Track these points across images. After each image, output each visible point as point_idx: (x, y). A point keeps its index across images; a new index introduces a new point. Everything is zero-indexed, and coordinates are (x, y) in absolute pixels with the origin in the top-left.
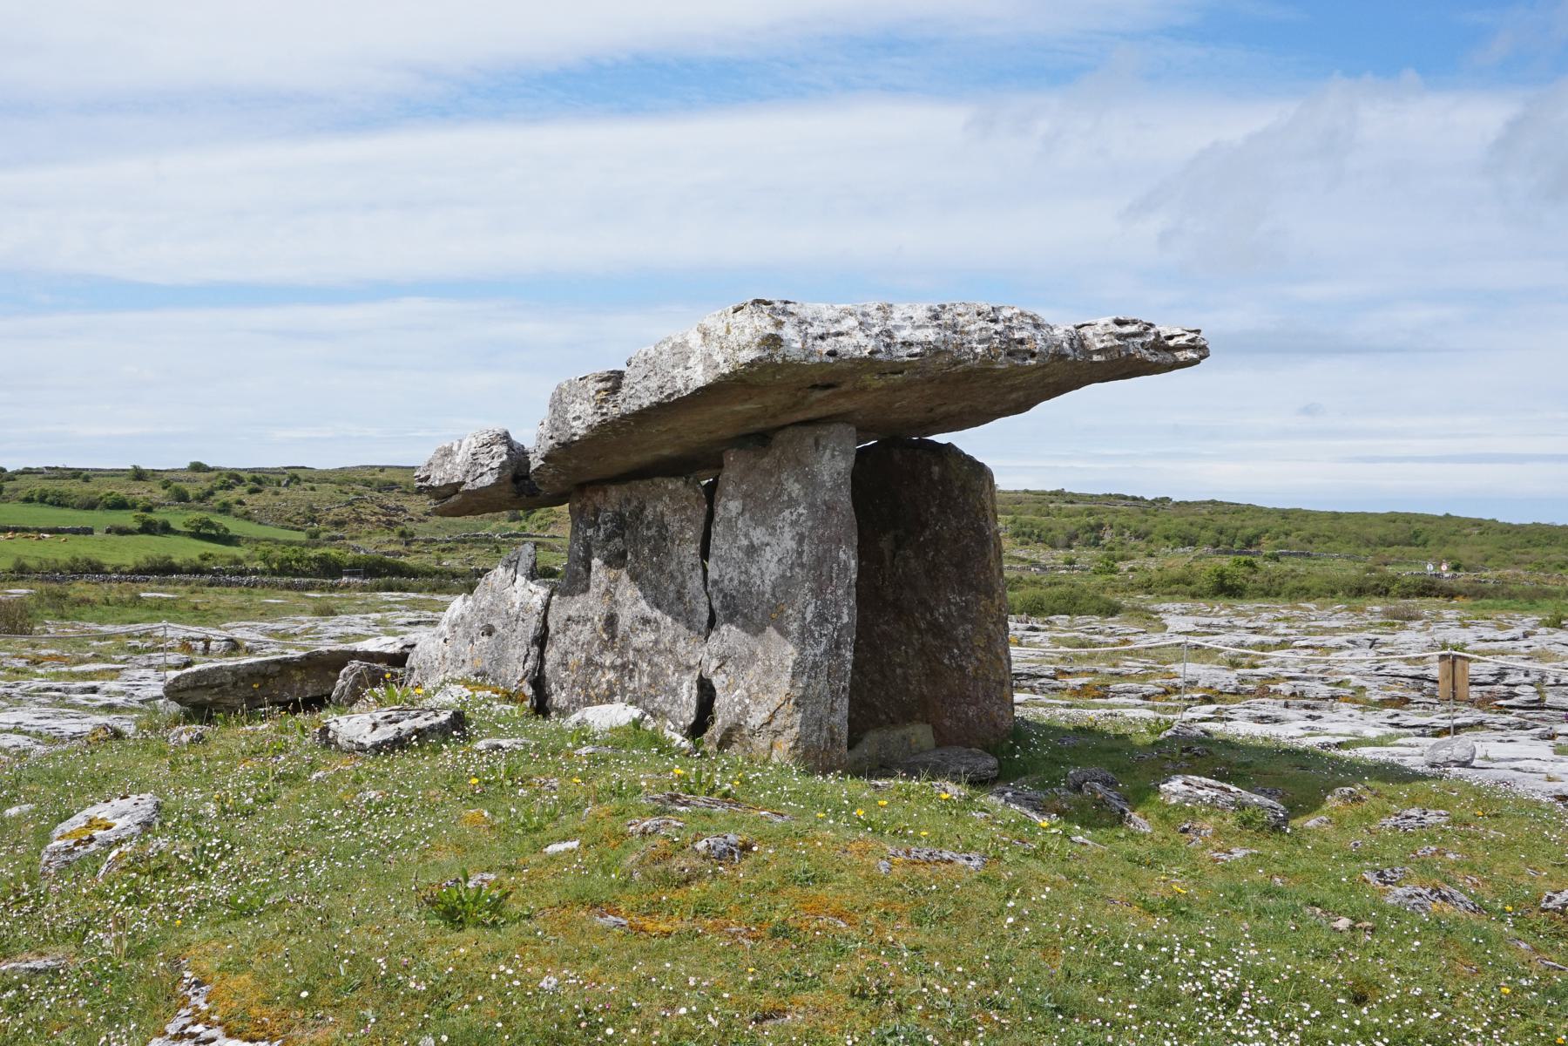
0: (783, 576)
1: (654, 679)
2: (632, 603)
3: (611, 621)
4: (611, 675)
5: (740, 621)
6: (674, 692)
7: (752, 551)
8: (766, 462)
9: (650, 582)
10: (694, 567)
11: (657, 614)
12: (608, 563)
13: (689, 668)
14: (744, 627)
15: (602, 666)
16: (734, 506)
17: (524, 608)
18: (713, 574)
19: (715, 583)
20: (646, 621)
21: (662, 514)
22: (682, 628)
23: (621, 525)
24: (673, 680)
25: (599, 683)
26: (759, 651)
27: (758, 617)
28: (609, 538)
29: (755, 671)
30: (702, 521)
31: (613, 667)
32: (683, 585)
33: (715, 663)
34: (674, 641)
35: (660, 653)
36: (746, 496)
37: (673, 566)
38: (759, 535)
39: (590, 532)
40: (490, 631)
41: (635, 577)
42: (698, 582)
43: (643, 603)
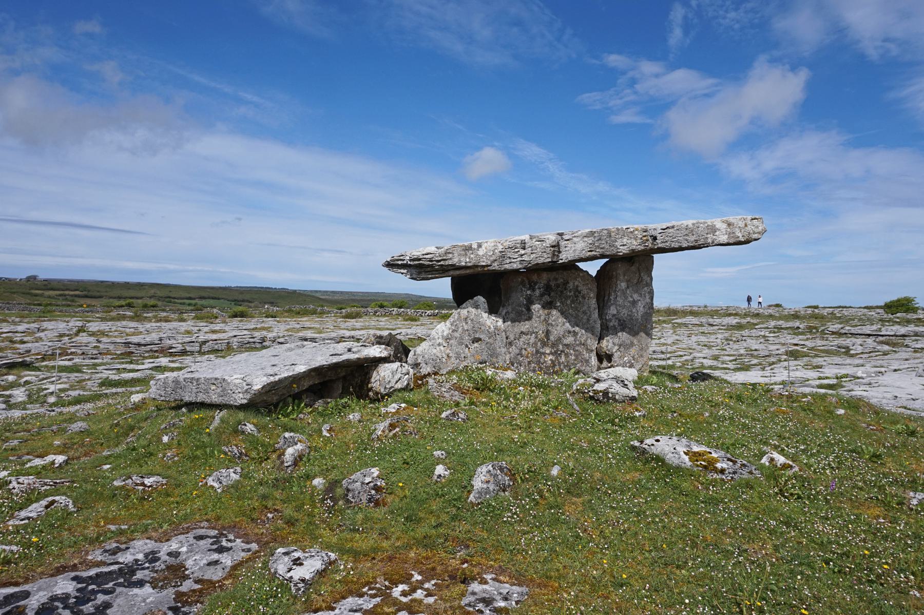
0: (646, 313)
1: (576, 356)
2: (560, 325)
3: (548, 333)
4: (551, 357)
5: (627, 330)
6: (587, 361)
7: (634, 303)
8: (633, 268)
9: (572, 315)
10: (595, 309)
11: (577, 329)
12: (544, 307)
13: (592, 351)
14: (629, 333)
15: (544, 354)
16: (624, 285)
17: (496, 328)
18: (613, 310)
19: (614, 315)
20: (569, 332)
21: (577, 286)
22: (590, 335)
23: (548, 289)
24: (587, 356)
25: (545, 362)
26: (635, 342)
27: (636, 328)
28: (542, 295)
29: (633, 351)
30: (596, 290)
31: (551, 353)
32: (590, 316)
33: (617, 347)
34: (586, 341)
35: (578, 345)
36: (628, 281)
37: (585, 308)
38: (636, 296)
39: (529, 292)
40: (477, 340)
41: (562, 313)
42: (597, 315)
43: (568, 324)
